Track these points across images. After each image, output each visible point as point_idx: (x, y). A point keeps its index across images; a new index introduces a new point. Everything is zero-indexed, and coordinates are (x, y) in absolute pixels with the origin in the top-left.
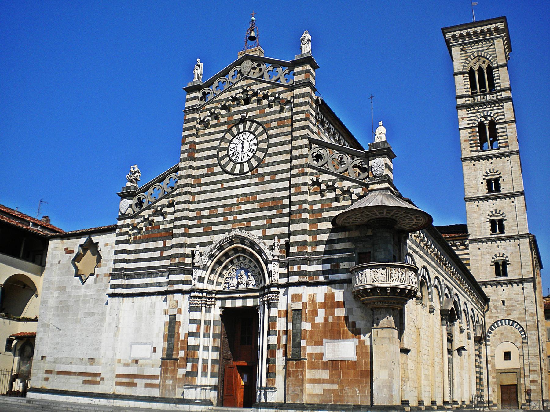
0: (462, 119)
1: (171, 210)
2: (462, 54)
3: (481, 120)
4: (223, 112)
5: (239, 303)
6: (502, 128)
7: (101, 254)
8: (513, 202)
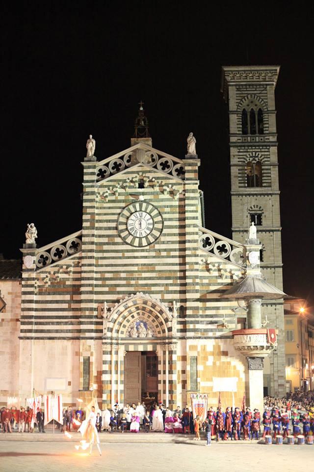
0: (234, 156)
1: (78, 269)
2: (238, 94)
3: (249, 159)
5: (141, 348)
6: (267, 169)
7: (5, 301)
8: (271, 236)
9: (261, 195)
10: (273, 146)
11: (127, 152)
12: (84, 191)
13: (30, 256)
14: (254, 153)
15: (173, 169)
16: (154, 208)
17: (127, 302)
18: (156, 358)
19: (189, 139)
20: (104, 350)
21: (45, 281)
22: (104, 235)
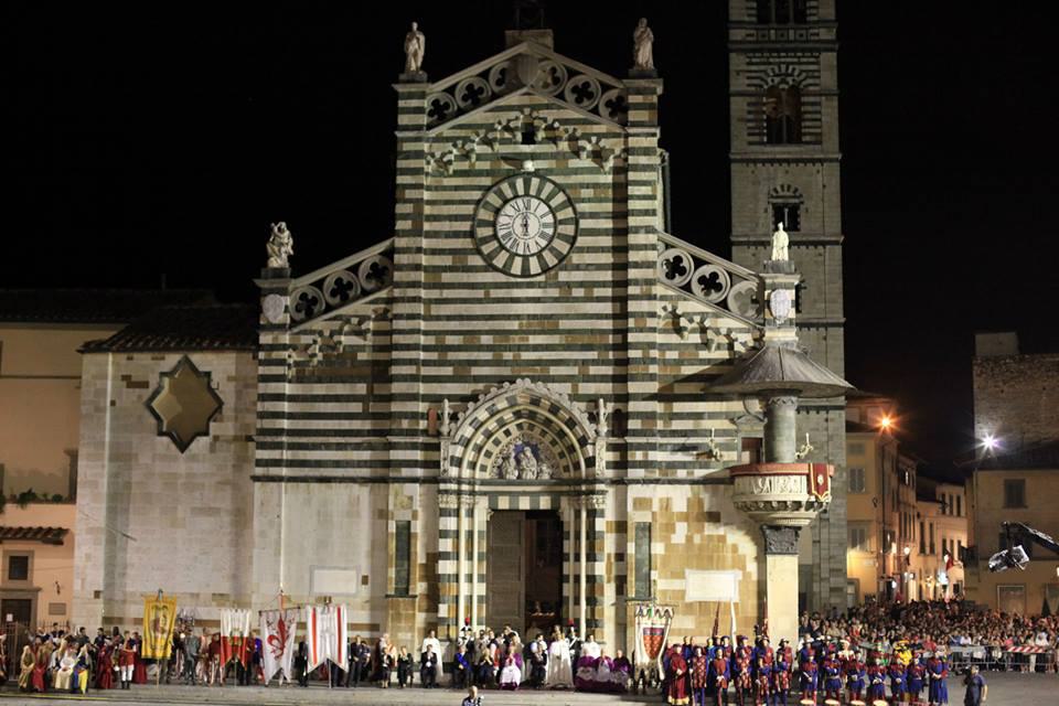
0: (738, 73)
1: (384, 325)
3: (773, 81)
4: (479, 149)
5: (525, 504)
6: (813, 104)
7: (221, 396)
8: (820, 255)
9: (797, 161)
10: (827, 50)
11: (497, 61)
12: (399, 149)
13: (278, 296)
14: (783, 67)
15: (601, 101)
16: (557, 189)
17: (495, 400)
18: (559, 524)
19: (637, 34)
20: (442, 506)
21: (309, 352)
22: (445, 250)
